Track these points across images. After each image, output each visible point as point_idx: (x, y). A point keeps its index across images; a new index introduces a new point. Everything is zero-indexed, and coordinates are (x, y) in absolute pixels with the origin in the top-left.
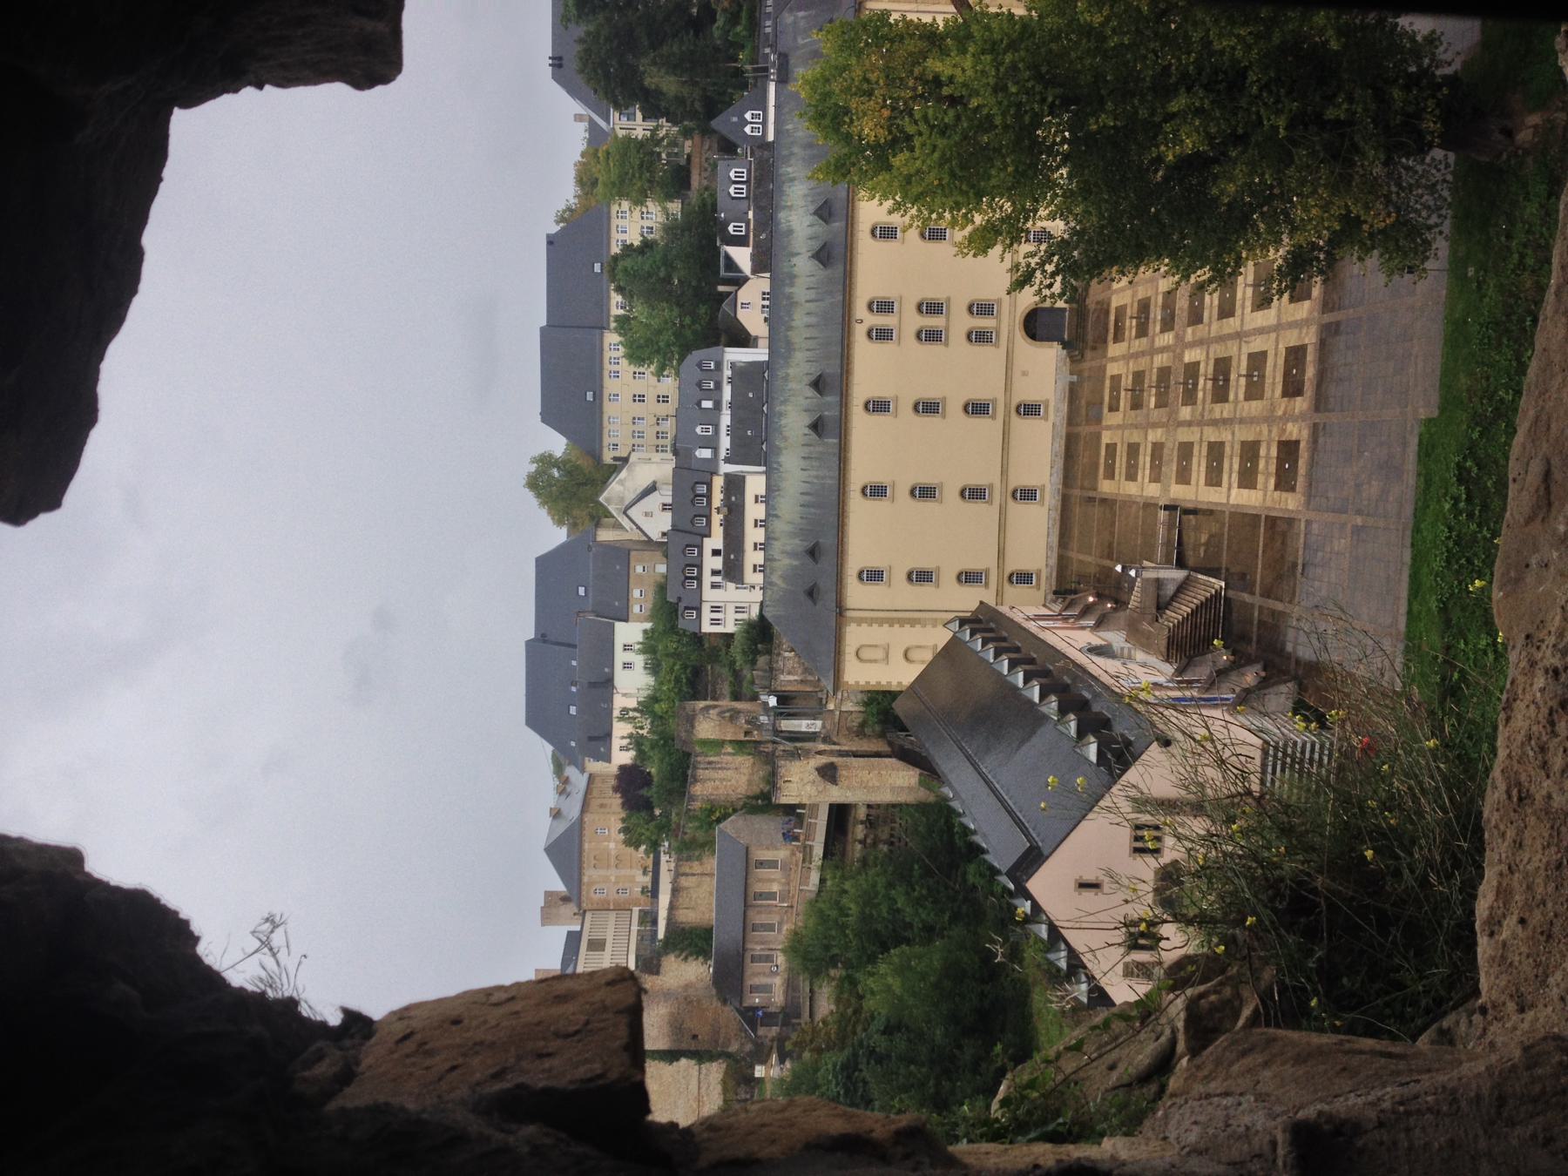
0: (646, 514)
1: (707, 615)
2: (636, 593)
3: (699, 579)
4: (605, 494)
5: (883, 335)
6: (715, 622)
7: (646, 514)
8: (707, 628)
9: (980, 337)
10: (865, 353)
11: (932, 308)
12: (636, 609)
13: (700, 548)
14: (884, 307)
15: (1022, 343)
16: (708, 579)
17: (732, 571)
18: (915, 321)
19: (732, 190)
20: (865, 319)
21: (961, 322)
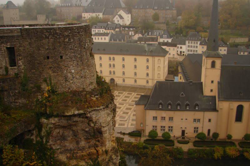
0: (117, 18)
1: (94, 29)
2: (107, 16)
3: (99, 28)
4: (122, 11)
5: (110, 59)
6: (93, 31)
7: (117, 18)
8: (92, 30)
9: (110, 73)
10: (108, 56)
11: (114, 66)
12: (105, 16)
13: (104, 28)
14: (114, 59)
15: (110, 78)
16: (99, 30)
17: (97, 34)
18: (112, 63)
19: (150, 33)
20: (112, 56)
21: (112, 70)
